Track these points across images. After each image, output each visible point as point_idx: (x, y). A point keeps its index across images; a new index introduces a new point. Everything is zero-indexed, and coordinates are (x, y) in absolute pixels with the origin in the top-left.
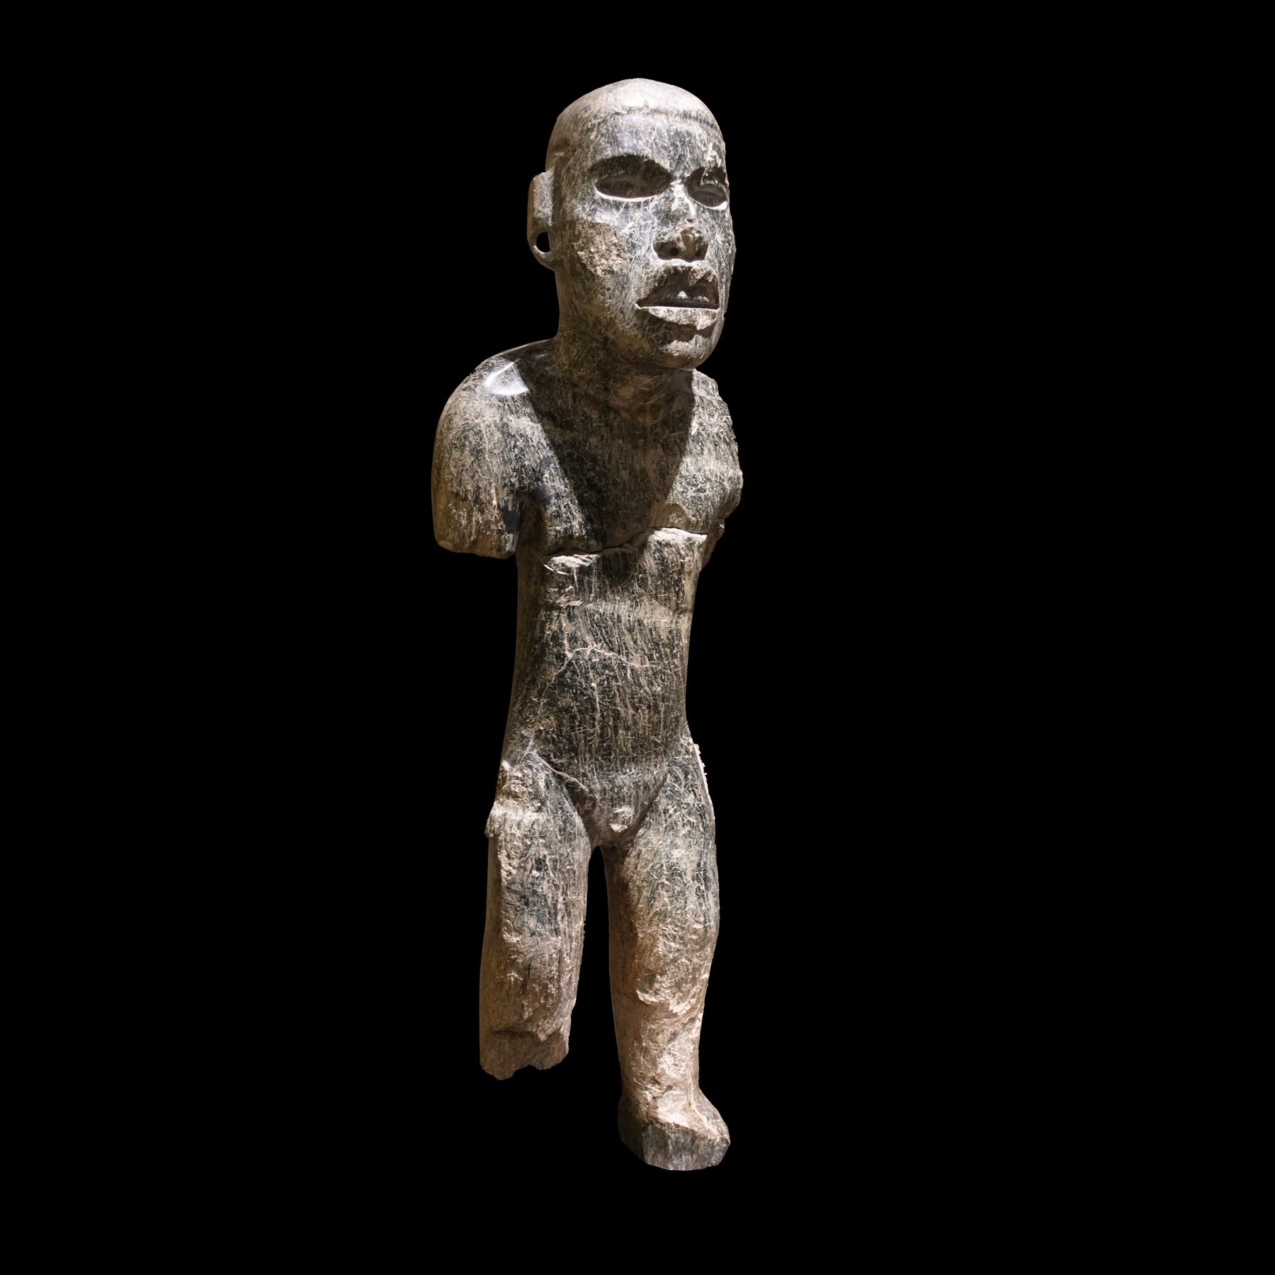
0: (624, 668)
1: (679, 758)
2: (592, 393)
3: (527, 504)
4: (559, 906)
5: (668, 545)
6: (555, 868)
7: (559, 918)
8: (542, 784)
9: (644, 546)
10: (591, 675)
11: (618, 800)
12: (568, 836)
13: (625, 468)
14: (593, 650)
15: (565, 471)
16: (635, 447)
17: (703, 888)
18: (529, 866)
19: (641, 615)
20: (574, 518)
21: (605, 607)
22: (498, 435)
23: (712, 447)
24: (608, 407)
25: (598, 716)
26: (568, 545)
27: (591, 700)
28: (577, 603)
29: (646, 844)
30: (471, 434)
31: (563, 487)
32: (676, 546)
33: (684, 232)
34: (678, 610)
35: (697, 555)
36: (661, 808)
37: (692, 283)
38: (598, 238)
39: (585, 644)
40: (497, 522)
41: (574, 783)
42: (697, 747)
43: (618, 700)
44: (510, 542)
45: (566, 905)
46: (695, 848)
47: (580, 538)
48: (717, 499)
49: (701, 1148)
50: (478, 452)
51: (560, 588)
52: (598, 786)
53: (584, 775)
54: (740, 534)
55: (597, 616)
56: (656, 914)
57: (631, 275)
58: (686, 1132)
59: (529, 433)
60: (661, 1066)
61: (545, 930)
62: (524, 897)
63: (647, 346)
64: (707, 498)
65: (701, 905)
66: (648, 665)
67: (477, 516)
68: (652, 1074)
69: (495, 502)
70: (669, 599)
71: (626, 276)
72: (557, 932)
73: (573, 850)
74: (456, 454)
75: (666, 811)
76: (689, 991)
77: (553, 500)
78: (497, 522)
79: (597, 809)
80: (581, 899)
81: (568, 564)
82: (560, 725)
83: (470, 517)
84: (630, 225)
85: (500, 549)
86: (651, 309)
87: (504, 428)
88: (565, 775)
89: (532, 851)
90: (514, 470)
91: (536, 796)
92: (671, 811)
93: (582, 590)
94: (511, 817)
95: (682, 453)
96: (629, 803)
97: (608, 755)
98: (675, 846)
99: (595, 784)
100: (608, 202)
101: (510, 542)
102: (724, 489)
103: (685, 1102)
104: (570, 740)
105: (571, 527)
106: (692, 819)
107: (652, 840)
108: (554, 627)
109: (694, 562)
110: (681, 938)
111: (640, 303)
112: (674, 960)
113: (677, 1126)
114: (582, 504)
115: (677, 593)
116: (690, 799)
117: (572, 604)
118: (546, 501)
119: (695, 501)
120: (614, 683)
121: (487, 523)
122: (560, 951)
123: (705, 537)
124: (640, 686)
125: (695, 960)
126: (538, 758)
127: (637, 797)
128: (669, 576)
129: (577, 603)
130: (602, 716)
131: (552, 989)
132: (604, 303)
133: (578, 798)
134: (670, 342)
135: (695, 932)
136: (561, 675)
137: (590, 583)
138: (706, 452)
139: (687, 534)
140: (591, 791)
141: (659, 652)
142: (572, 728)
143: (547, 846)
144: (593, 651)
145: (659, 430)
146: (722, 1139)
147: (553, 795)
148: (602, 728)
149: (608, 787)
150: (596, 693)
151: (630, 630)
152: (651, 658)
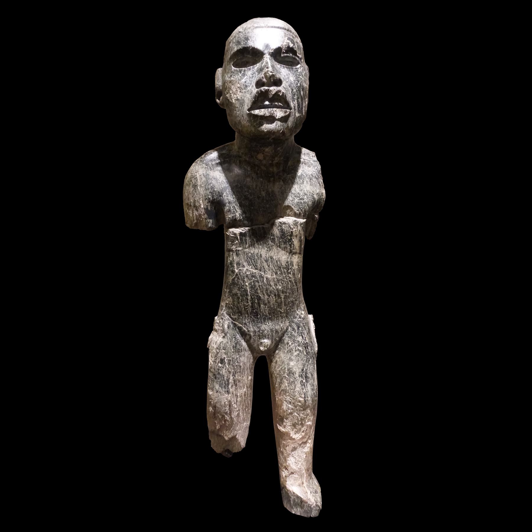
0: (263, 277)
1: (296, 320)
2: (247, 159)
3: (216, 205)
4: (230, 381)
5: (284, 223)
6: (229, 364)
7: (230, 386)
8: (226, 326)
9: (273, 224)
10: (246, 280)
11: (262, 336)
12: (237, 349)
13: (264, 191)
14: (247, 269)
15: (234, 192)
16: (269, 181)
17: (304, 381)
18: (217, 361)
19: (272, 254)
20: (237, 211)
21: (254, 251)
22: (204, 179)
23: (308, 180)
24: (254, 165)
25: (249, 298)
26: (235, 224)
27: (246, 291)
28: (240, 249)
29: (279, 358)
30: (193, 179)
31: (232, 199)
32: (288, 224)
33: (265, 73)
34: (291, 253)
35: (299, 228)
36: (286, 342)
37: (270, 96)
38: (232, 87)
39: (244, 266)
40: (204, 214)
41: (241, 327)
42: (311, 317)
43: (259, 291)
44: (210, 223)
45: (234, 381)
46: (301, 362)
47: (240, 220)
48: (310, 203)
49: (305, 506)
50: (195, 186)
51: (232, 242)
52: (252, 329)
53: (245, 324)
54: (323, 219)
55: (250, 254)
56: (282, 390)
57: (245, 99)
58: (298, 497)
59: (218, 177)
60: (289, 462)
61: (223, 390)
62: (214, 375)
63: (253, 129)
64: (304, 203)
65: (303, 389)
66: (275, 276)
67: (196, 213)
68: (284, 465)
69: (202, 206)
70: (286, 248)
71: (244, 100)
72: (228, 392)
73: (240, 356)
74: (187, 188)
75: (288, 343)
76: (300, 429)
77: (227, 205)
78: (204, 214)
79: (252, 339)
80: (247, 378)
81: (235, 232)
82: (234, 301)
83: (193, 213)
84: (245, 78)
85: (207, 226)
86: (252, 112)
87: (206, 176)
88: (237, 323)
89: (219, 355)
90: (210, 192)
91: (223, 331)
92: (290, 344)
93: (242, 243)
94: (215, 339)
95: (293, 183)
96: (268, 338)
97: (256, 315)
98: (291, 359)
99: (251, 328)
100: (237, 71)
101: (210, 223)
102: (314, 199)
103: (300, 482)
104: (238, 308)
105: (235, 215)
106: (300, 348)
107: (281, 356)
108: (231, 259)
109: (298, 230)
110: (294, 403)
111: (249, 110)
112: (291, 413)
113: (294, 493)
114: (241, 206)
115: (290, 245)
116: (300, 339)
117: (238, 249)
118: (224, 205)
119: (298, 204)
120: (257, 284)
121: (200, 215)
122: (230, 401)
123: (305, 220)
124: (271, 286)
125: (301, 415)
126: (226, 315)
127: (272, 336)
128: (286, 239)
129: (240, 249)
130: (251, 298)
131: (227, 417)
132: (236, 113)
133: (243, 334)
134: (262, 125)
135: (300, 401)
136: (233, 280)
137: (246, 240)
138: (305, 182)
139: (295, 219)
140: (248, 331)
141: (281, 271)
142: (238, 303)
143: (225, 353)
144: (247, 269)
145: (281, 174)
146: (317, 505)
147: (231, 331)
148: (252, 303)
149: (257, 330)
150: (248, 288)
151: (266, 261)
152: (276, 273)
